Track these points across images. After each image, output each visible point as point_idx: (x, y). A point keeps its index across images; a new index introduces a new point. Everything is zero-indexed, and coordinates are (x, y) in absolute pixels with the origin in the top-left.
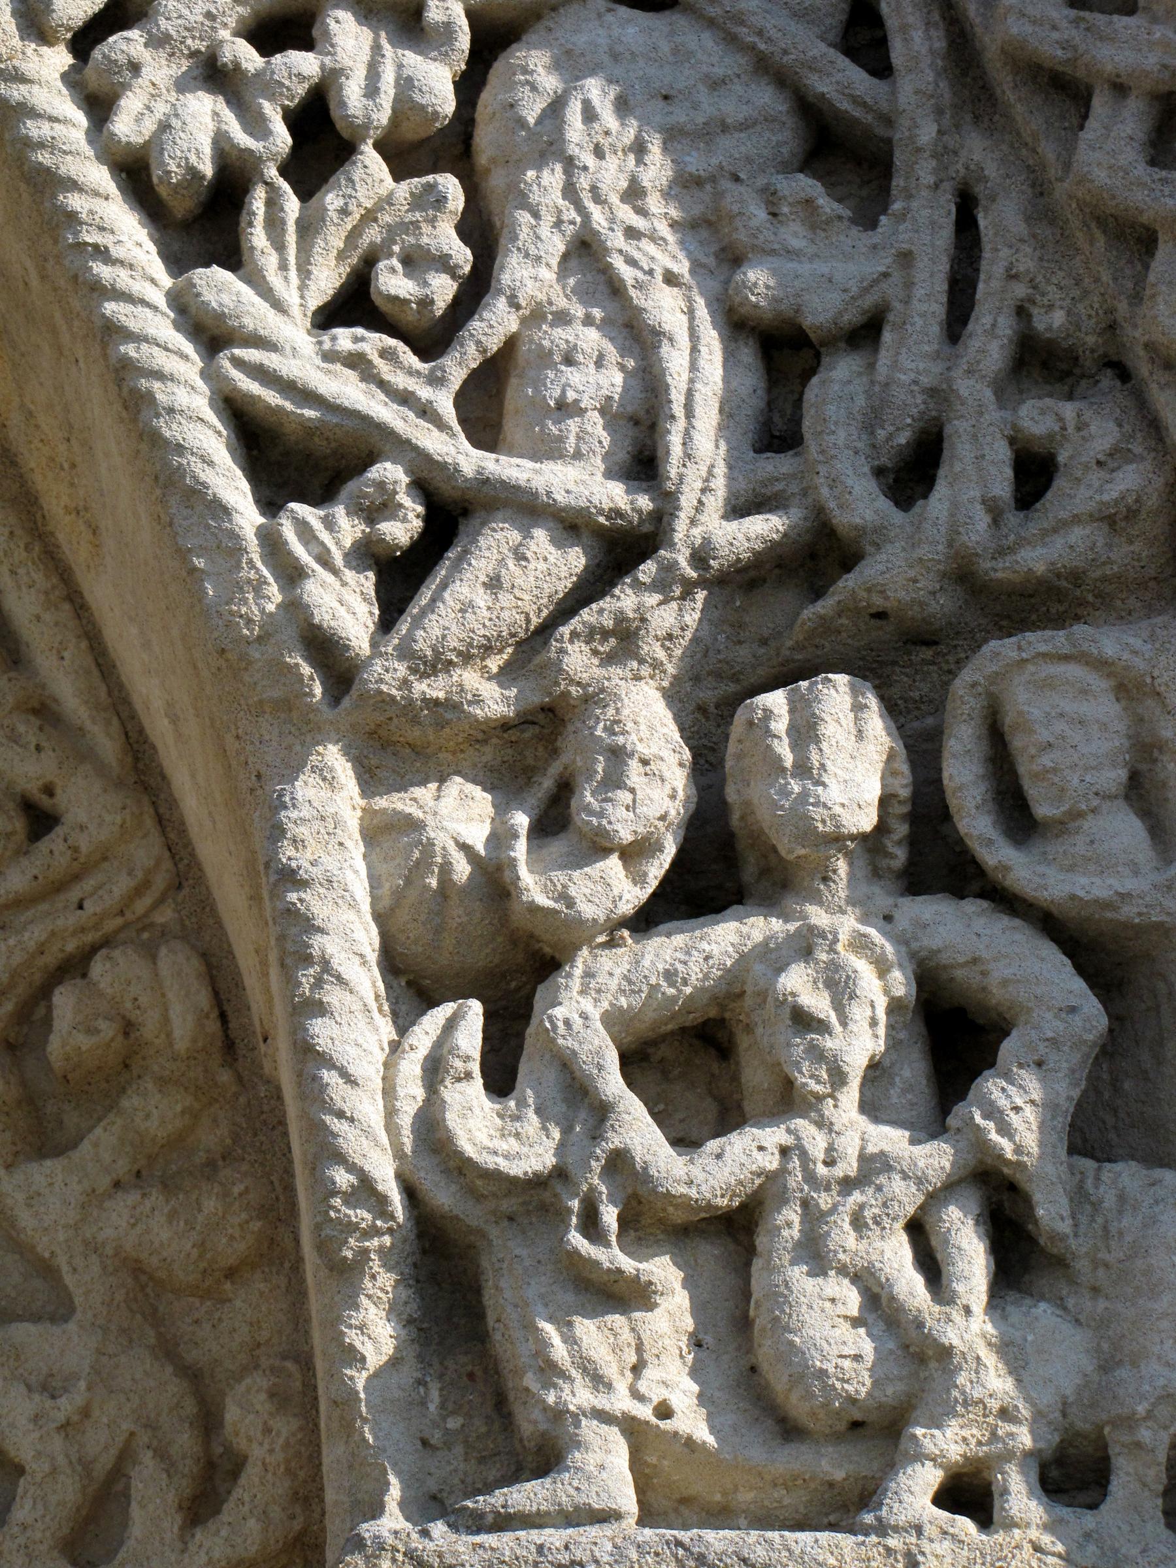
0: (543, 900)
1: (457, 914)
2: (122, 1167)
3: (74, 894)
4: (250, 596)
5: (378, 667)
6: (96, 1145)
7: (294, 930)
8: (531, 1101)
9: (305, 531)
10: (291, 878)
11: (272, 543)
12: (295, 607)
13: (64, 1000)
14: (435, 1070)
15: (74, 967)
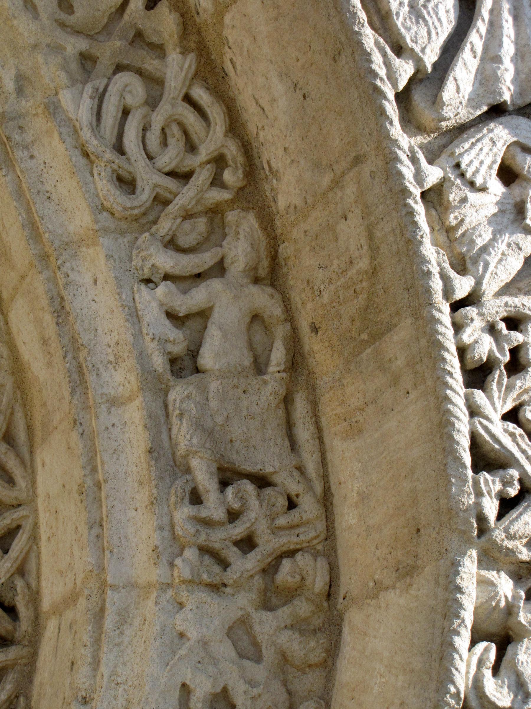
0: (523, 622)
1: (496, 615)
2: (289, 622)
3: (297, 531)
4: (466, 496)
5: (497, 532)
6: (283, 612)
7: (455, 606)
8: (506, 683)
9: (486, 481)
10: (459, 589)
11: (476, 483)
12: (478, 505)
13: (286, 564)
14: (481, 663)
15: (291, 554)
